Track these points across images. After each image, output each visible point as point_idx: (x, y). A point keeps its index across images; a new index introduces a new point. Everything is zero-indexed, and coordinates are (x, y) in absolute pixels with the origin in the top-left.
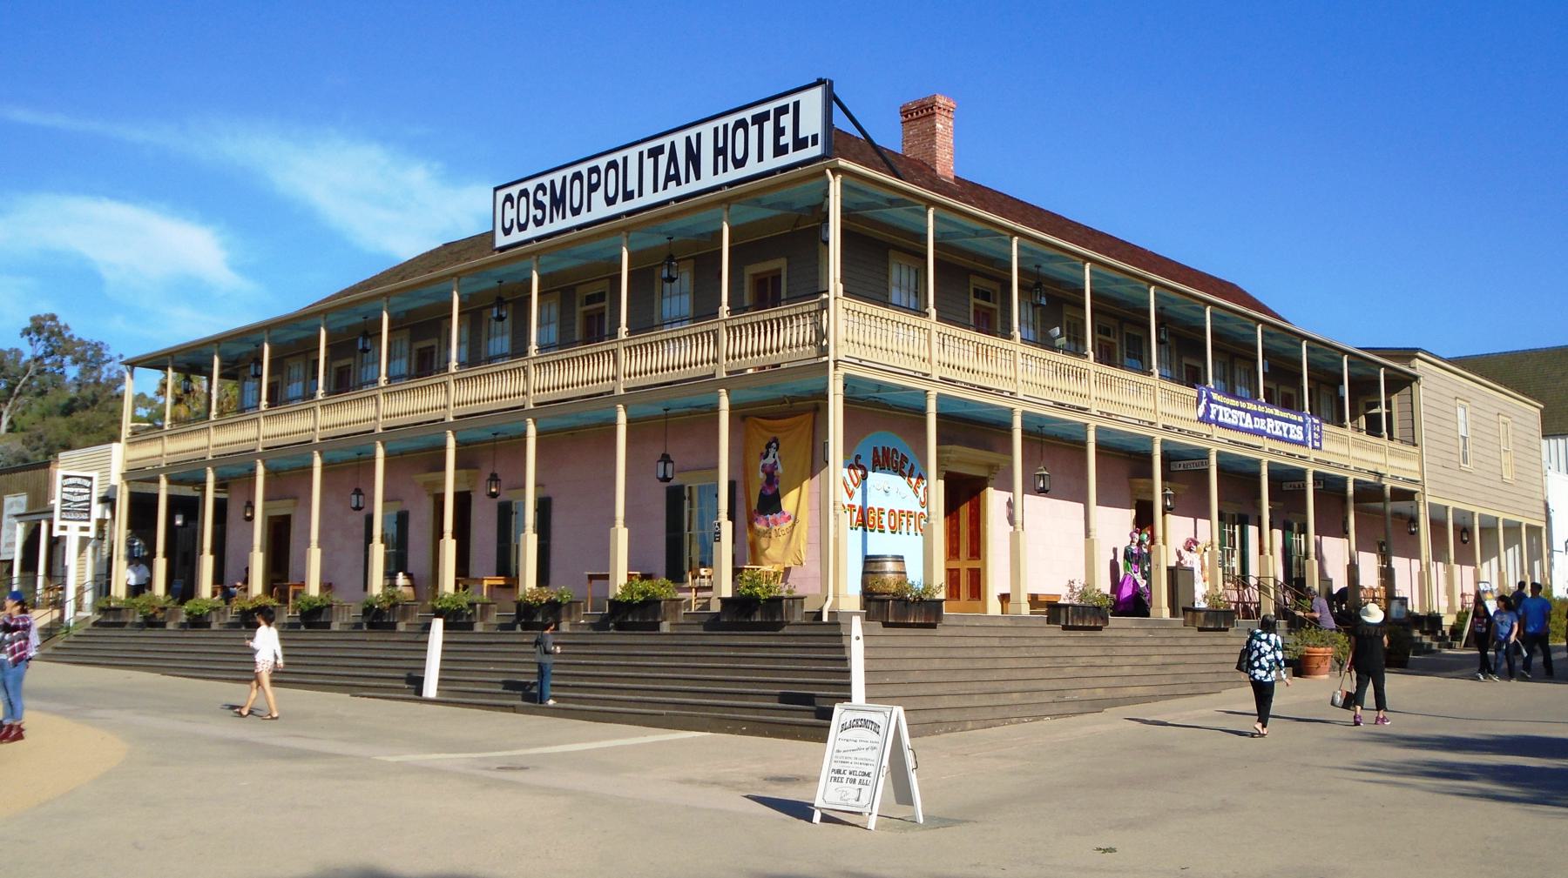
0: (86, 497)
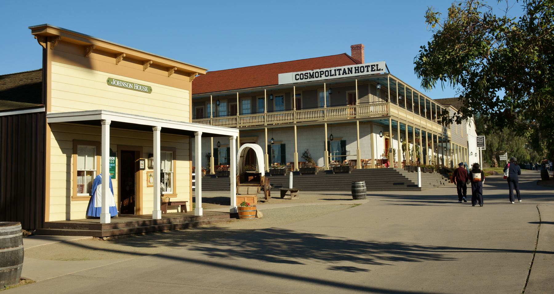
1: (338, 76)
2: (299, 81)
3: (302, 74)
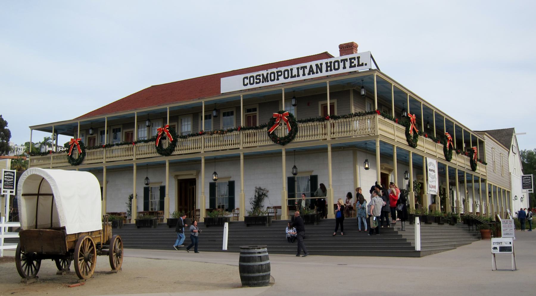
0: (12, 180)
1: (302, 78)
2: (249, 87)
3: (253, 77)
